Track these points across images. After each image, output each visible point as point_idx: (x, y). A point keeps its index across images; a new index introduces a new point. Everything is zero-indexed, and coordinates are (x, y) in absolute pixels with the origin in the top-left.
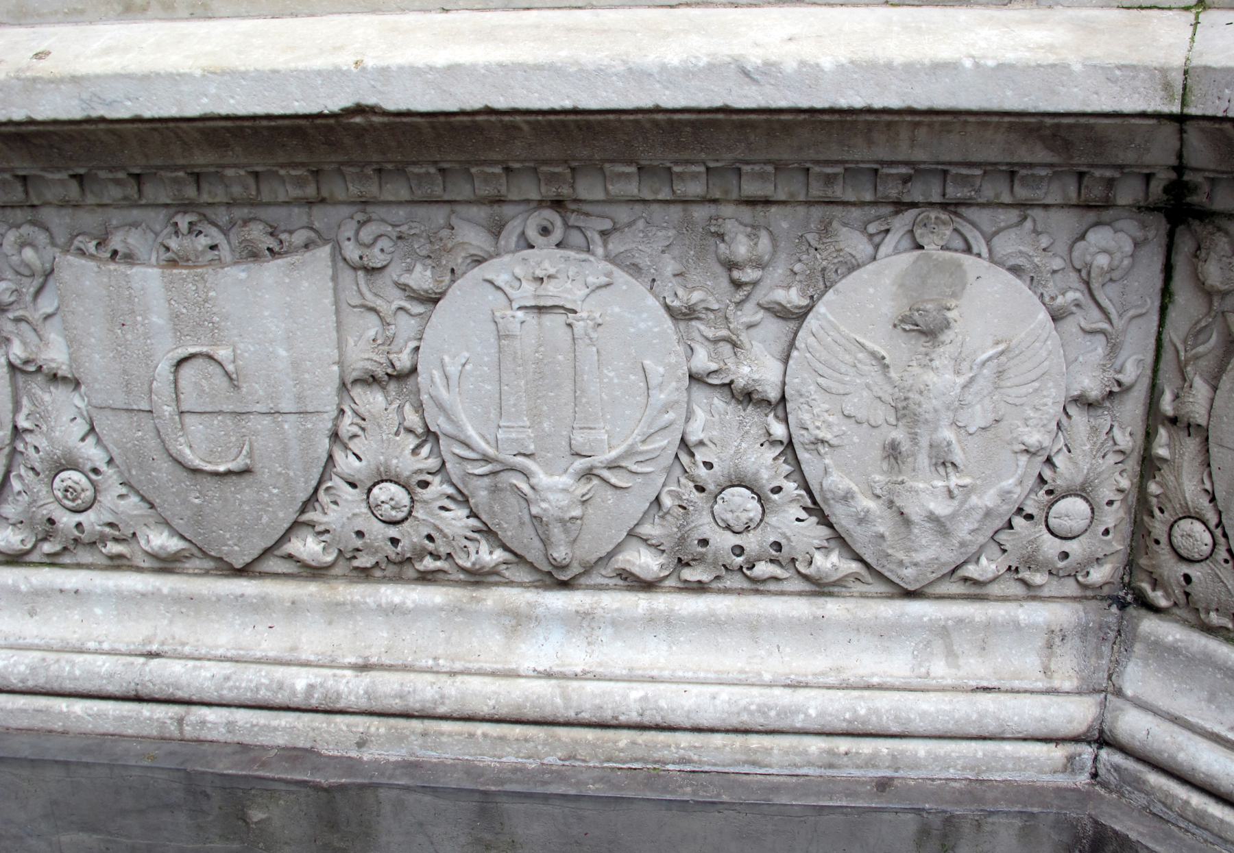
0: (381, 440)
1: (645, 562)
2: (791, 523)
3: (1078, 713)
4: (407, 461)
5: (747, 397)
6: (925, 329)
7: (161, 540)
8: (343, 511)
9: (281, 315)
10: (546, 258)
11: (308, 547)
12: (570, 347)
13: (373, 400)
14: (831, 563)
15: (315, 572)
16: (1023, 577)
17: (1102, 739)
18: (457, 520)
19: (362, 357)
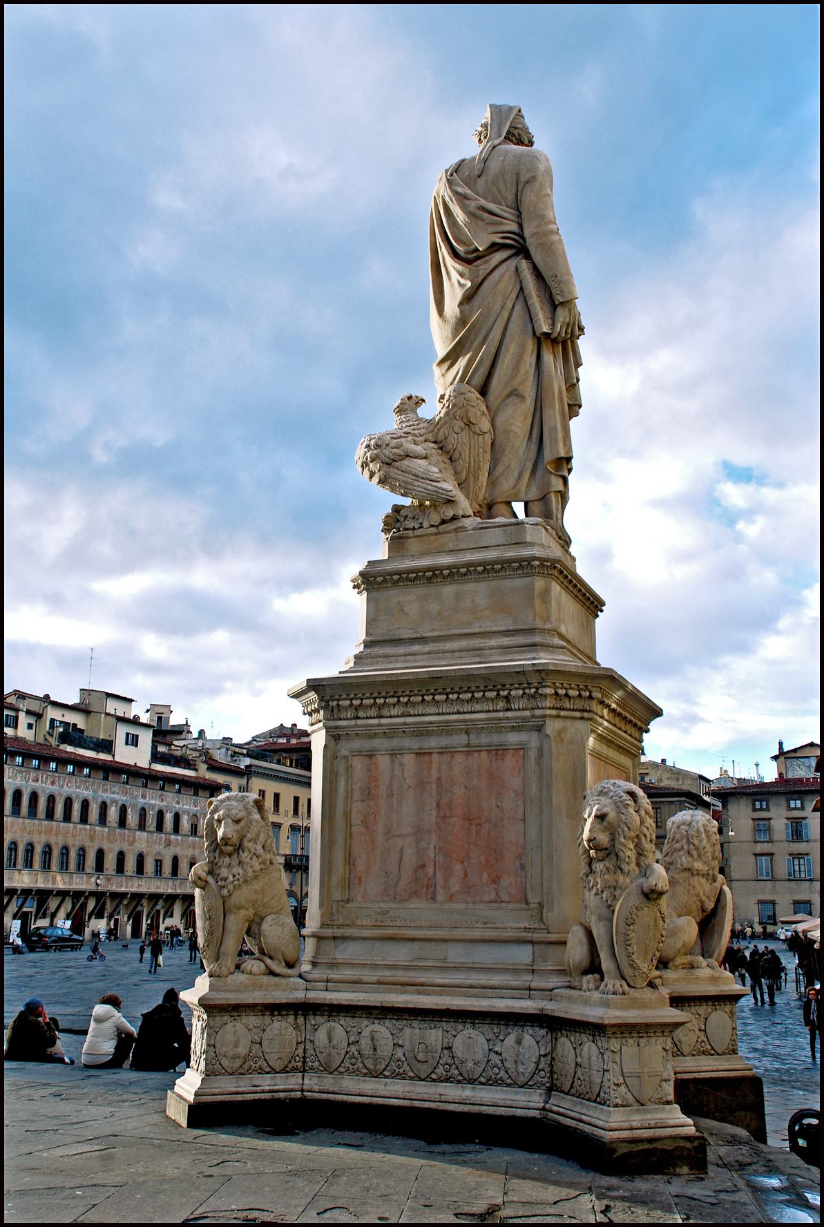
0: (446, 1058)
1: (482, 1080)
2: (502, 1073)
3: (542, 1105)
4: (450, 1061)
5: (497, 1053)
6: (519, 1042)
7: (411, 1074)
8: (440, 1070)
9: (435, 1035)
10: (471, 1031)
11: (434, 1076)
12: (471, 1043)
13: (446, 1052)
14: (509, 1081)
15: (434, 1080)
16: (538, 1085)
17: (543, 1109)
18: (456, 1072)
19: (445, 1045)
